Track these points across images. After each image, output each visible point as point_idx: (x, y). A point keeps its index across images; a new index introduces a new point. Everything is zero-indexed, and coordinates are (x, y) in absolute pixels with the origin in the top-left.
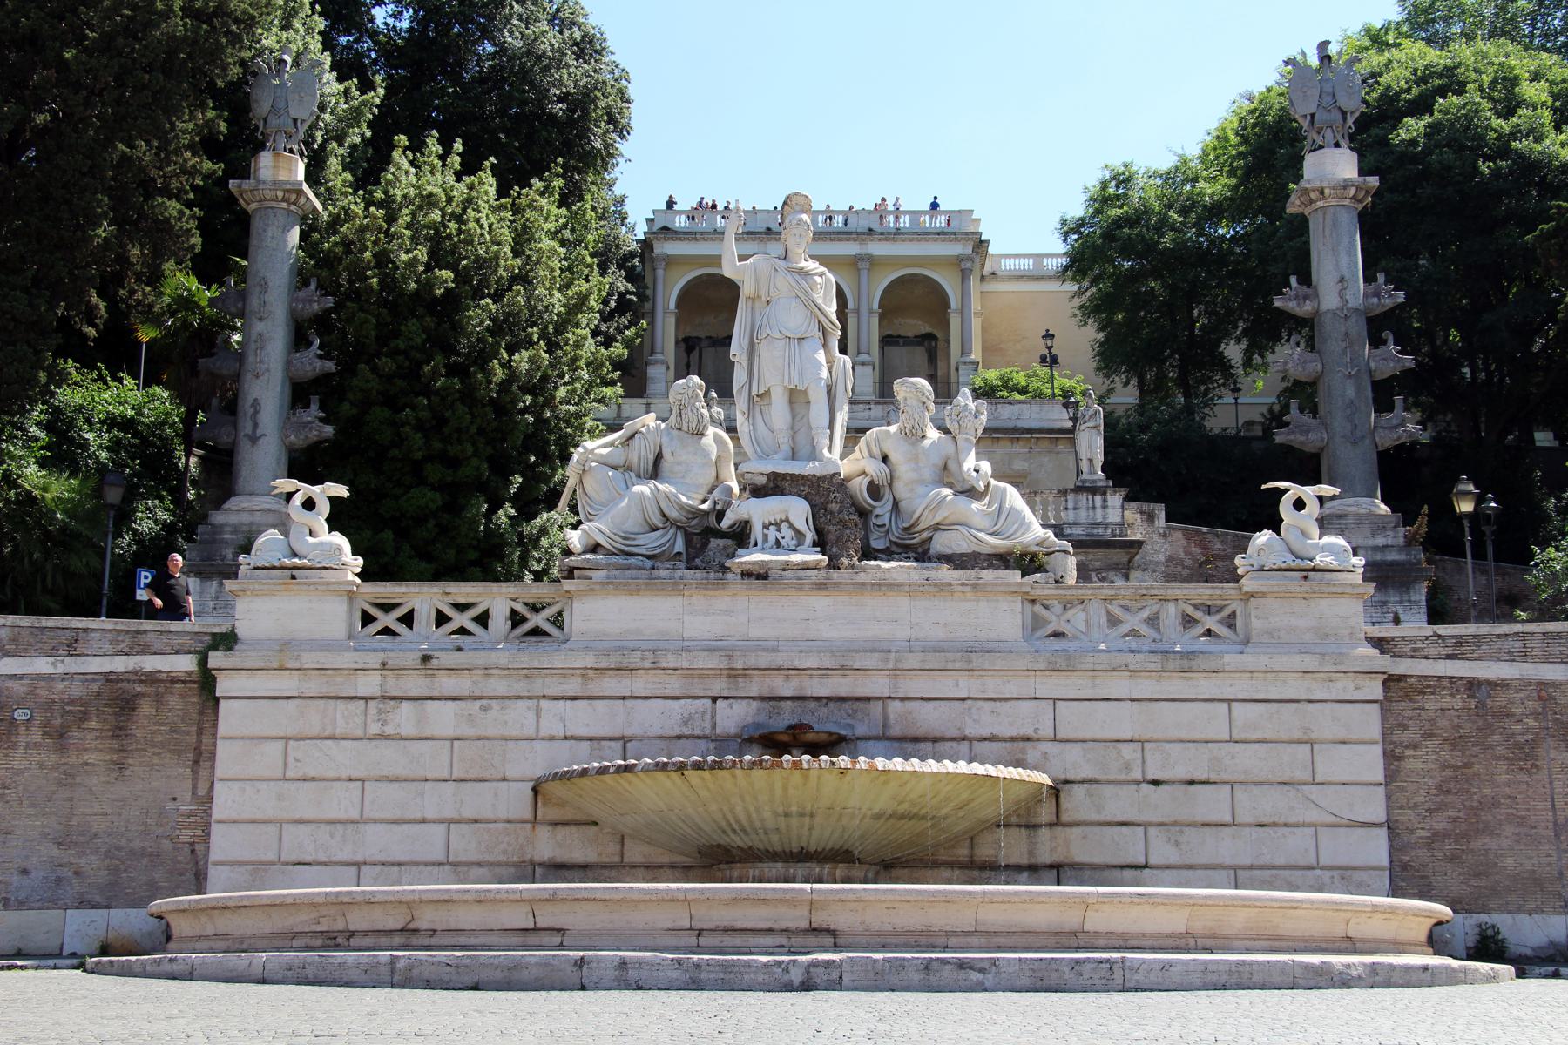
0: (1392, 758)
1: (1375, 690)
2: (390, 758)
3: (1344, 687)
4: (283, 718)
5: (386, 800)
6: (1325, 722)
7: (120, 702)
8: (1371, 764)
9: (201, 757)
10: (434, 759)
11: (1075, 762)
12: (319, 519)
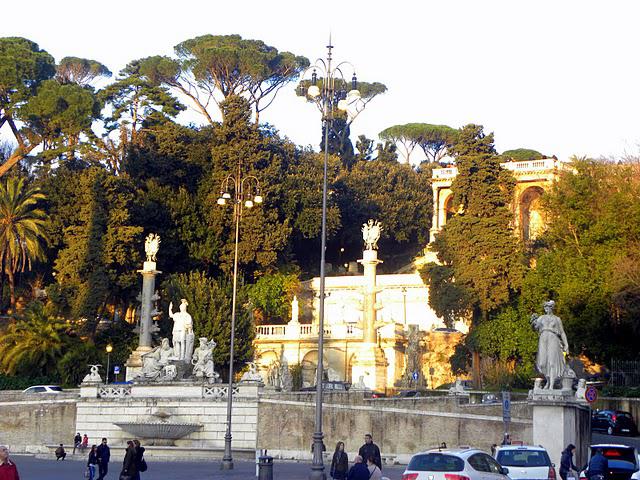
0: (259, 419)
1: (256, 405)
2: (101, 418)
3: (251, 405)
4: (87, 411)
5: (101, 426)
6: (248, 411)
7: (62, 407)
8: (254, 419)
9: (75, 418)
10: (108, 418)
11: (204, 419)
12: (96, 372)
